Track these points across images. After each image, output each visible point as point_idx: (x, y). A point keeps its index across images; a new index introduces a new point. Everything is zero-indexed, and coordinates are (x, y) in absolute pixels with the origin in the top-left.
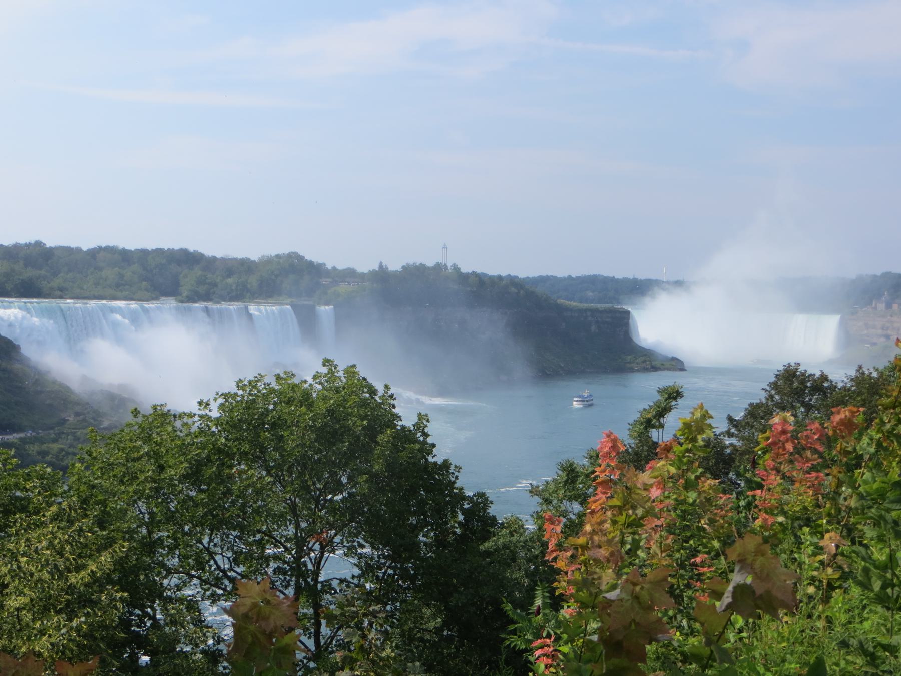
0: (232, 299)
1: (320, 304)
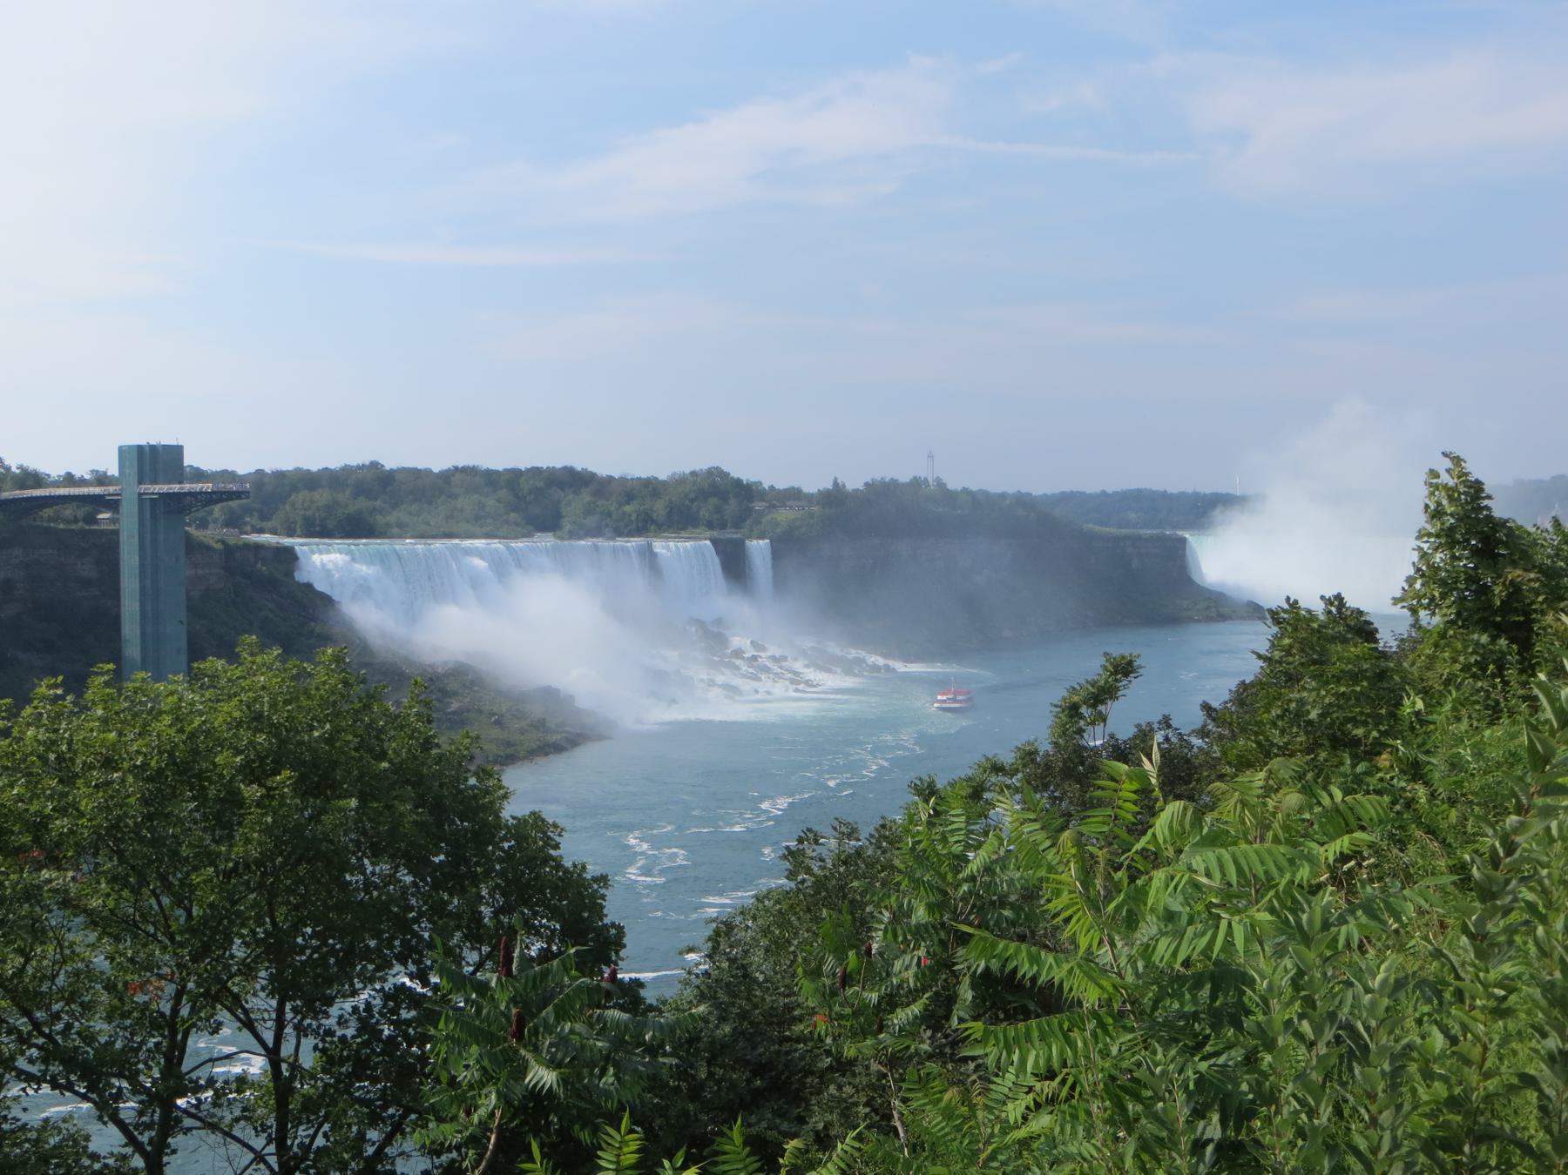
0: (630, 534)
1: (750, 537)
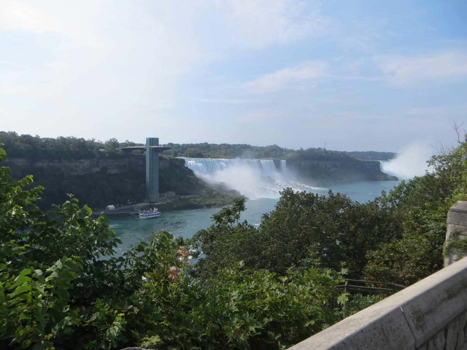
0: (256, 159)
